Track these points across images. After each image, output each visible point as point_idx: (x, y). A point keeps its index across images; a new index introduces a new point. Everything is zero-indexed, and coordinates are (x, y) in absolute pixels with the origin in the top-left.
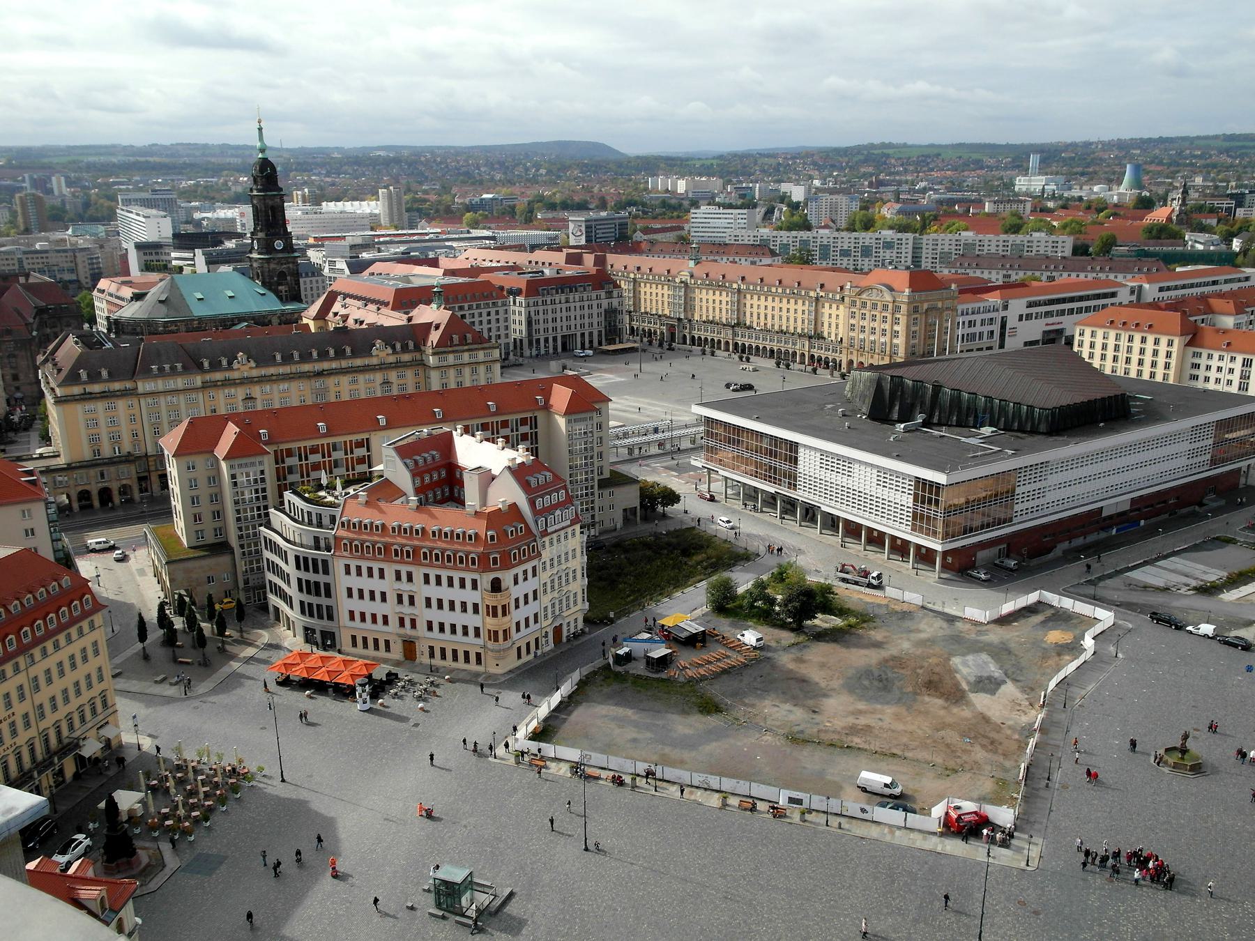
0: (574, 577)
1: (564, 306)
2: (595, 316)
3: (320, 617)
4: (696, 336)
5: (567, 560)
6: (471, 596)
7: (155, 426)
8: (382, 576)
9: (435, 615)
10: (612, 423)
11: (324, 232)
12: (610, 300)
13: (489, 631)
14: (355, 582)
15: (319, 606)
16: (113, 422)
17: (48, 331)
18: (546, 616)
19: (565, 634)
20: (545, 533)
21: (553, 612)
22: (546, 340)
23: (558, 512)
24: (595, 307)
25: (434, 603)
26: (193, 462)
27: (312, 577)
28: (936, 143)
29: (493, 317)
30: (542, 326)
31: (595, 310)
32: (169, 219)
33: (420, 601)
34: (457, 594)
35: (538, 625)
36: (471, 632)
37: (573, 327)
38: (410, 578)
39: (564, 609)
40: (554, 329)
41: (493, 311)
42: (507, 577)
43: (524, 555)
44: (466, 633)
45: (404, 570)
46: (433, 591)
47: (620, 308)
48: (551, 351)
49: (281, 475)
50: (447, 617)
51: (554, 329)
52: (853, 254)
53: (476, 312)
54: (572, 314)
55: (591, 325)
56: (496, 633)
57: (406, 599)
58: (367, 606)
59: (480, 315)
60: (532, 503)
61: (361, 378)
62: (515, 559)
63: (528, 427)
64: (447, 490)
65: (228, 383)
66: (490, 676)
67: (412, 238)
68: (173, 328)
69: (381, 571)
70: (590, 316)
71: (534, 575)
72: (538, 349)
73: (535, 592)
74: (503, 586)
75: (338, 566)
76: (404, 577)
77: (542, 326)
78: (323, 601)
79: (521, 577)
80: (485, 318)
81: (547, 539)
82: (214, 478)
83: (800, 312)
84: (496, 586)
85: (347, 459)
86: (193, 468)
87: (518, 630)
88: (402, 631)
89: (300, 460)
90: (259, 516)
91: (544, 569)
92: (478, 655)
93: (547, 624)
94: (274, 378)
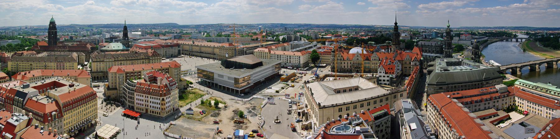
0: (177, 98)
6: (159, 101)
8: (143, 96)
14: (138, 97)
15: (131, 101)
19: (175, 109)
20: (172, 90)
23: (174, 86)
27: (131, 96)
29: (160, 51)
30: (168, 53)
33: (149, 102)
34: (156, 101)
36: (158, 108)
40: (170, 53)
42: (165, 98)
44: (157, 108)
45: (147, 95)
46: (152, 100)
50: (154, 105)
53: (157, 50)
58: (140, 102)
60: (169, 84)
66: (162, 117)
71: (170, 98)
75: (136, 93)
77: (168, 53)
78: (132, 100)
80: (158, 51)
84: (163, 100)
87: (167, 108)
88: (145, 107)
93: (172, 107)
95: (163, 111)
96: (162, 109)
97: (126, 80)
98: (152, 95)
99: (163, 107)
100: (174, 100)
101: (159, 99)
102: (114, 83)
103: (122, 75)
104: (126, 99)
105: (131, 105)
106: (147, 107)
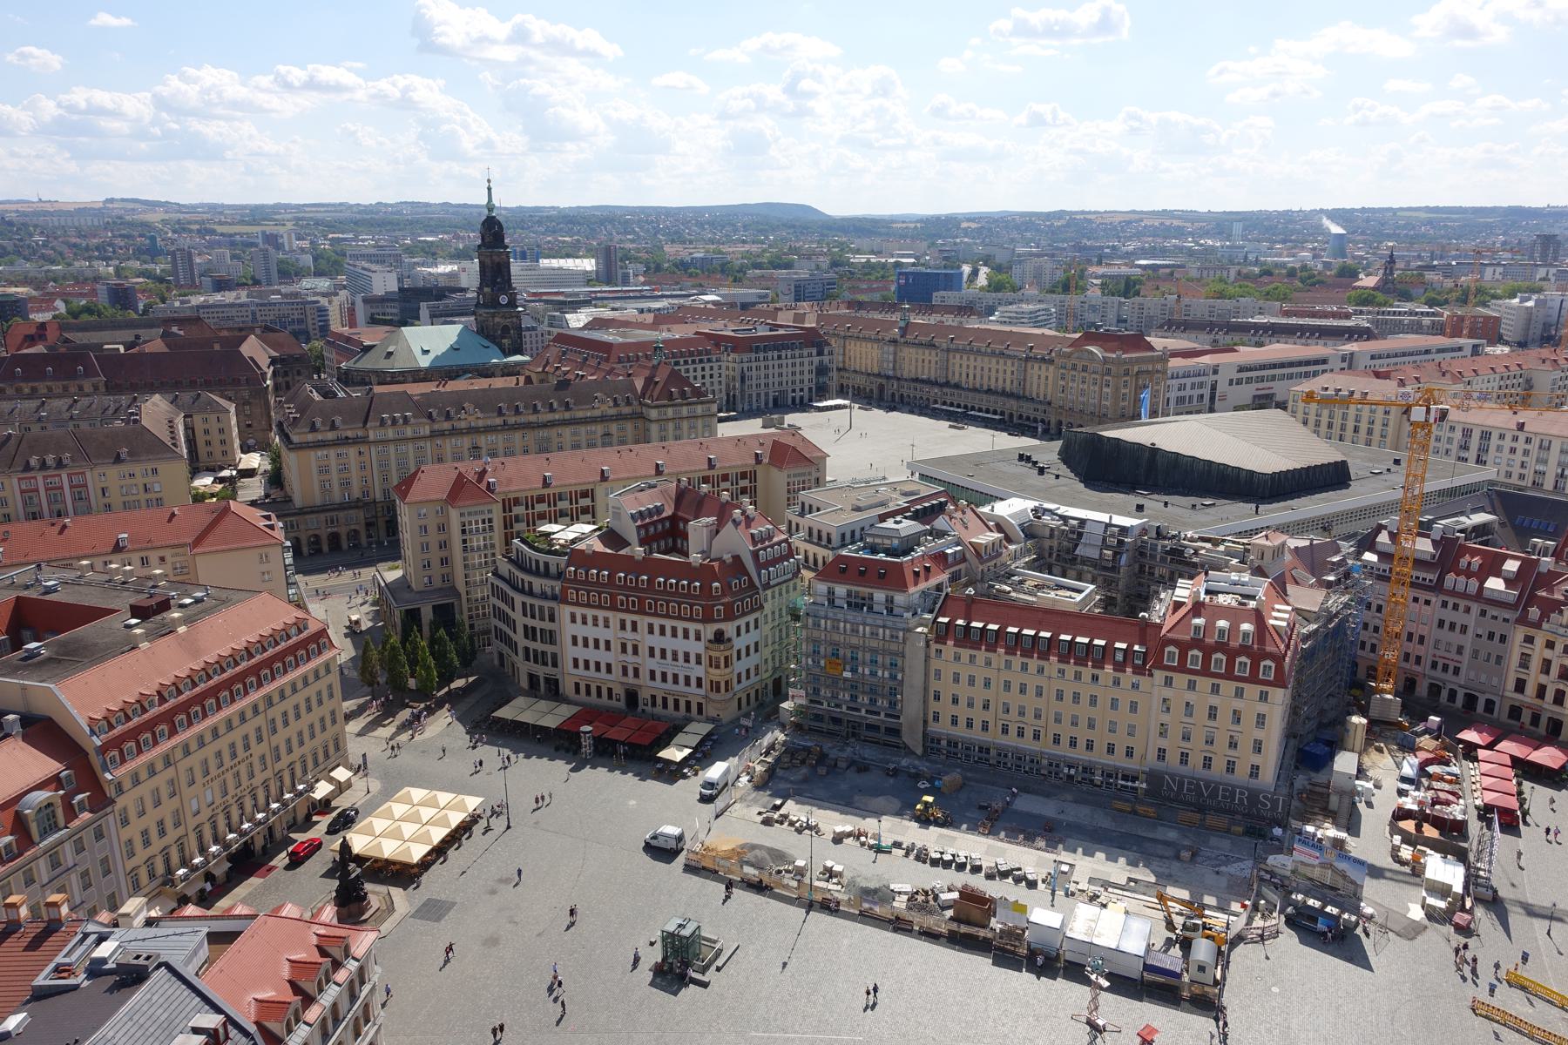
2: (806, 372)
6: (696, 647)
10: (828, 479)
11: (545, 287)
14: (580, 631)
16: (344, 469)
17: (280, 380)
20: (767, 586)
22: (758, 395)
24: (806, 364)
25: (657, 653)
27: (537, 623)
28: (1138, 209)
29: (707, 373)
31: (806, 368)
34: (680, 645)
35: (758, 678)
36: (693, 682)
38: (634, 628)
40: (767, 385)
42: (729, 628)
45: (629, 618)
46: (657, 641)
47: (830, 366)
48: (763, 406)
49: (508, 524)
51: (767, 385)
54: (784, 370)
56: (718, 683)
57: (630, 649)
58: (592, 655)
59: (695, 370)
60: (755, 555)
61: (583, 429)
64: (670, 541)
65: (455, 432)
68: (401, 379)
69: (606, 621)
70: (802, 373)
73: (756, 644)
74: (726, 636)
76: (629, 626)
77: (754, 382)
81: (769, 592)
83: (1009, 373)
84: (719, 637)
87: (739, 682)
88: (625, 680)
89: (527, 508)
92: (700, 705)
97: (508, 543)
98: (656, 615)
100: (781, 638)
104: (513, 645)
105: (541, 671)
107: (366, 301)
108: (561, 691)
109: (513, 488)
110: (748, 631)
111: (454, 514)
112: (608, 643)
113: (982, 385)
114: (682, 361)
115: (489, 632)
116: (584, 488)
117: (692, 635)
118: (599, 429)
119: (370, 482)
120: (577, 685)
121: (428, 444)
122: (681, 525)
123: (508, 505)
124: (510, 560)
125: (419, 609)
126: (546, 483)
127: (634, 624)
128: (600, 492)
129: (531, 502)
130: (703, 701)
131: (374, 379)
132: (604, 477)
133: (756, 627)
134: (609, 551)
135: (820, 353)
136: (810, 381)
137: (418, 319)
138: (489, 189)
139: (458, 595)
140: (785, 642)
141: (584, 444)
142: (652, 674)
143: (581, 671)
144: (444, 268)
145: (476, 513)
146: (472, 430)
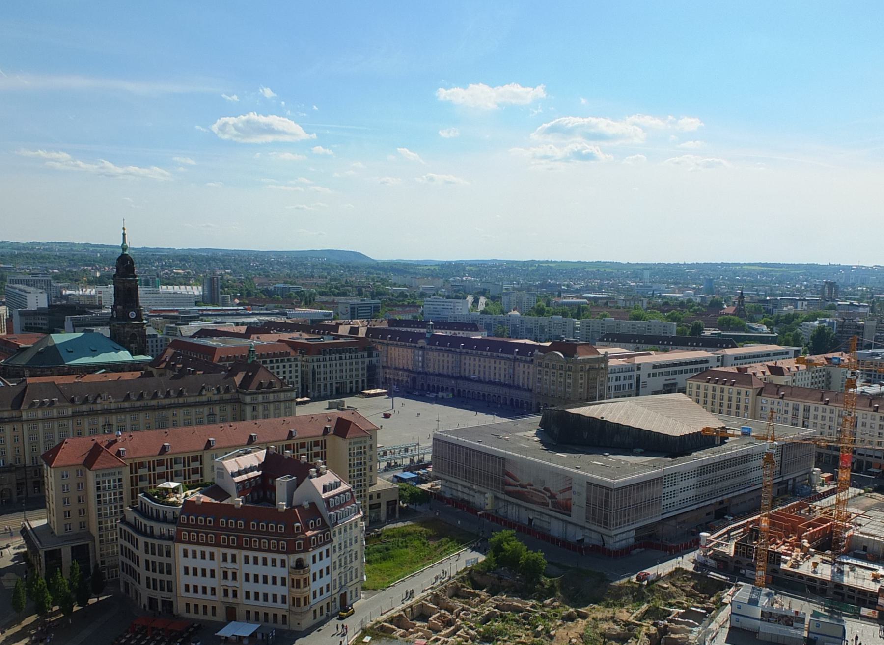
0: (356, 558)
1: (338, 362)
2: (360, 369)
3: (162, 589)
4: (431, 385)
5: (351, 544)
6: (280, 572)
7: (34, 444)
9: (251, 587)
10: (378, 445)
11: (164, 306)
12: (371, 359)
13: (293, 598)
14: (191, 563)
18: (335, 586)
21: (340, 583)
22: (325, 386)
24: (360, 363)
26: (67, 472)
29: (287, 369)
32: (45, 295)
33: (241, 577)
36: (279, 599)
37: (344, 377)
39: (348, 581)
40: (331, 378)
41: (293, 364)
43: (321, 541)
45: (229, 552)
46: (252, 569)
49: (134, 482)
50: (261, 588)
51: (331, 378)
52: (534, 331)
54: (344, 368)
55: (357, 376)
58: (200, 581)
61: (193, 411)
62: (314, 544)
63: (320, 447)
64: (262, 493)
65: (92, 413)
67: (227, 312)
70: (357, 370)
72: (319, 391)
73: (328, 568)
77: (322, 376)
78: (165, 577)
79: (318, 557)
82: (82, 484)
85: (185, 470)
86: (67, 476)
87: (315, 597)
88: (226, 600)
89: (150, 470)
90: (116, 513)
91: (335, 551)
94: (128, 410)
95: (298, 610)
96: (296, 602)
97: (134, 496)
98: (251, 549)
99: (297, 592)
100: (346, 563)
101: (283, 561)
102: (74, 513)
103: (114, 474)
104: (137, 576)
105: (159, 595)
106: (230, 599)
107: (21, 314)
108: (175, 612)
109: (138, 454)
110: (321, 559)
111: (91, 476)
112: (213, 572)
113: (484, 378)
114: (268, 360)
115: (117, 566)
116: (194, 454)
117: (279, 563)
118: (206, 410)
119: (21, 450)
120: (188, 605)
121: (71, 422)
122: (270, 481)
123: (133, 468)
124: (135, 510)
125: (60, 550)
126: (163, 450)
127: (234, 557)
128: (207, 456)
129: (152, 466)
130: (287, 614)
131: (27, 373)
132: (209, 445)
133: (327, 556)
134: (213, 501)
135: (370, 356)
136: (363, 375)
137: (63, 328)
138: (124, 234)
139: (93, 538)
140: (349, 566)
141: (194, 422)
142: (248, 595)
143: (191, 594)
144: (91, 291)
145: (108, 474)
146: (109, 412)
